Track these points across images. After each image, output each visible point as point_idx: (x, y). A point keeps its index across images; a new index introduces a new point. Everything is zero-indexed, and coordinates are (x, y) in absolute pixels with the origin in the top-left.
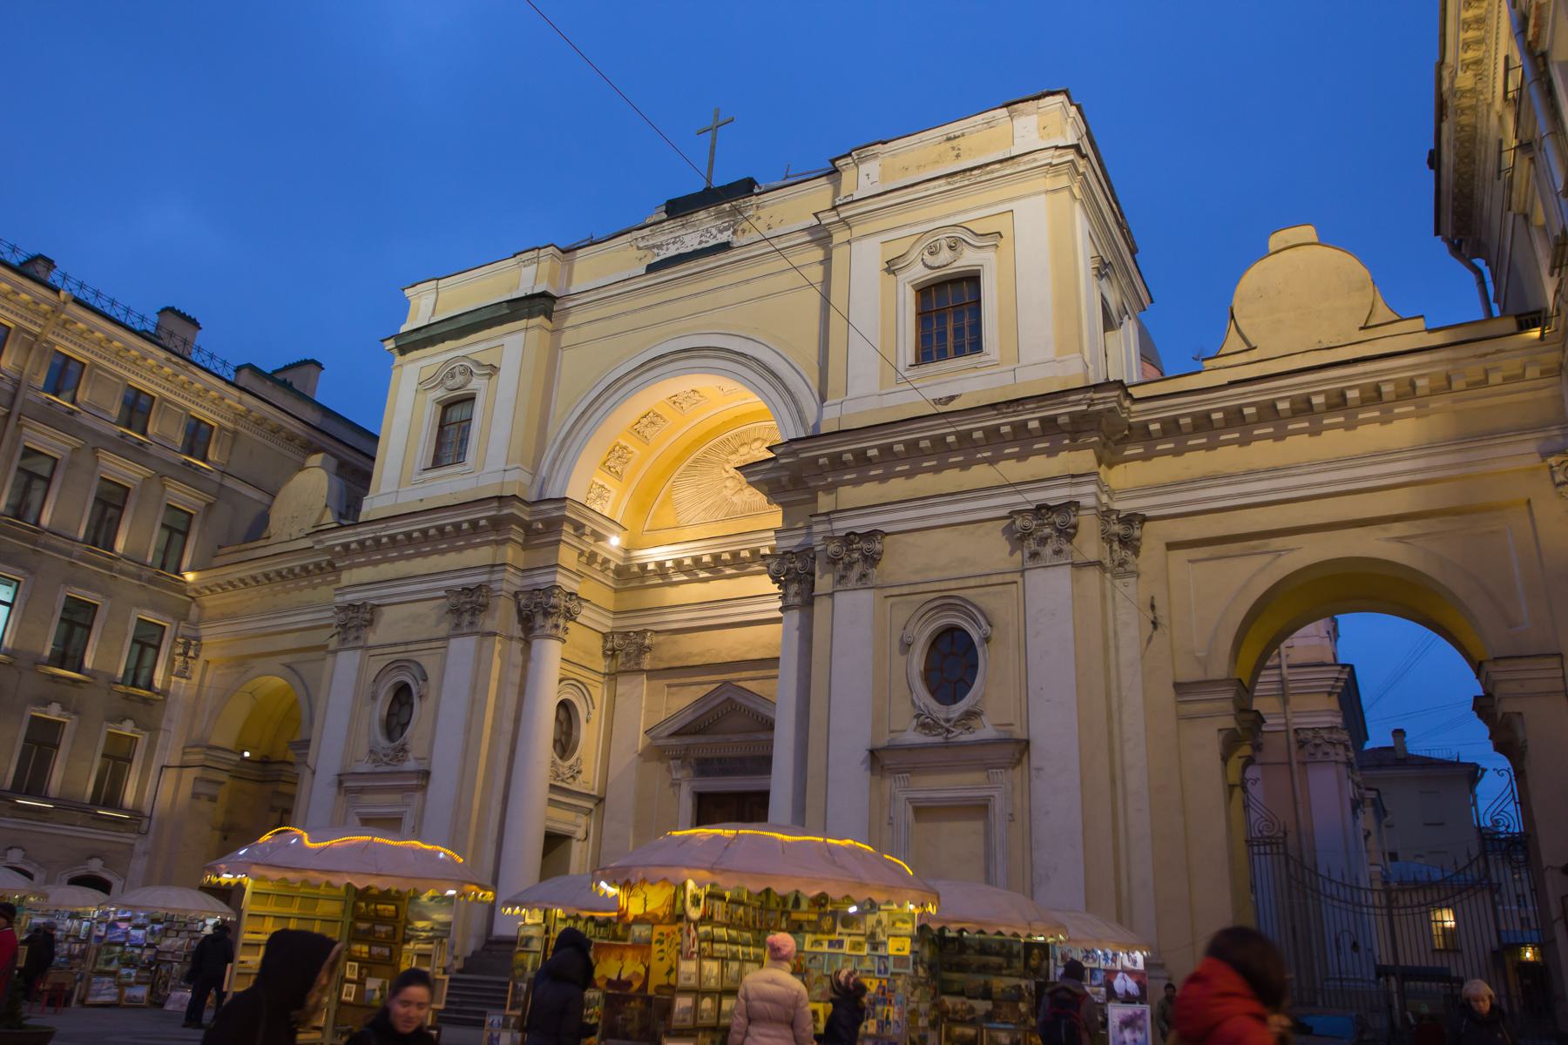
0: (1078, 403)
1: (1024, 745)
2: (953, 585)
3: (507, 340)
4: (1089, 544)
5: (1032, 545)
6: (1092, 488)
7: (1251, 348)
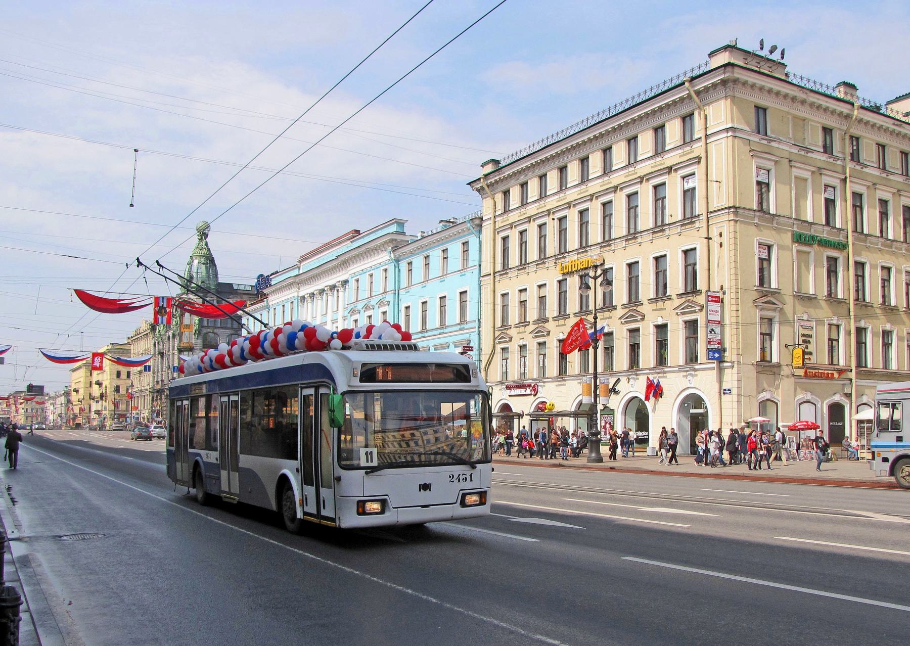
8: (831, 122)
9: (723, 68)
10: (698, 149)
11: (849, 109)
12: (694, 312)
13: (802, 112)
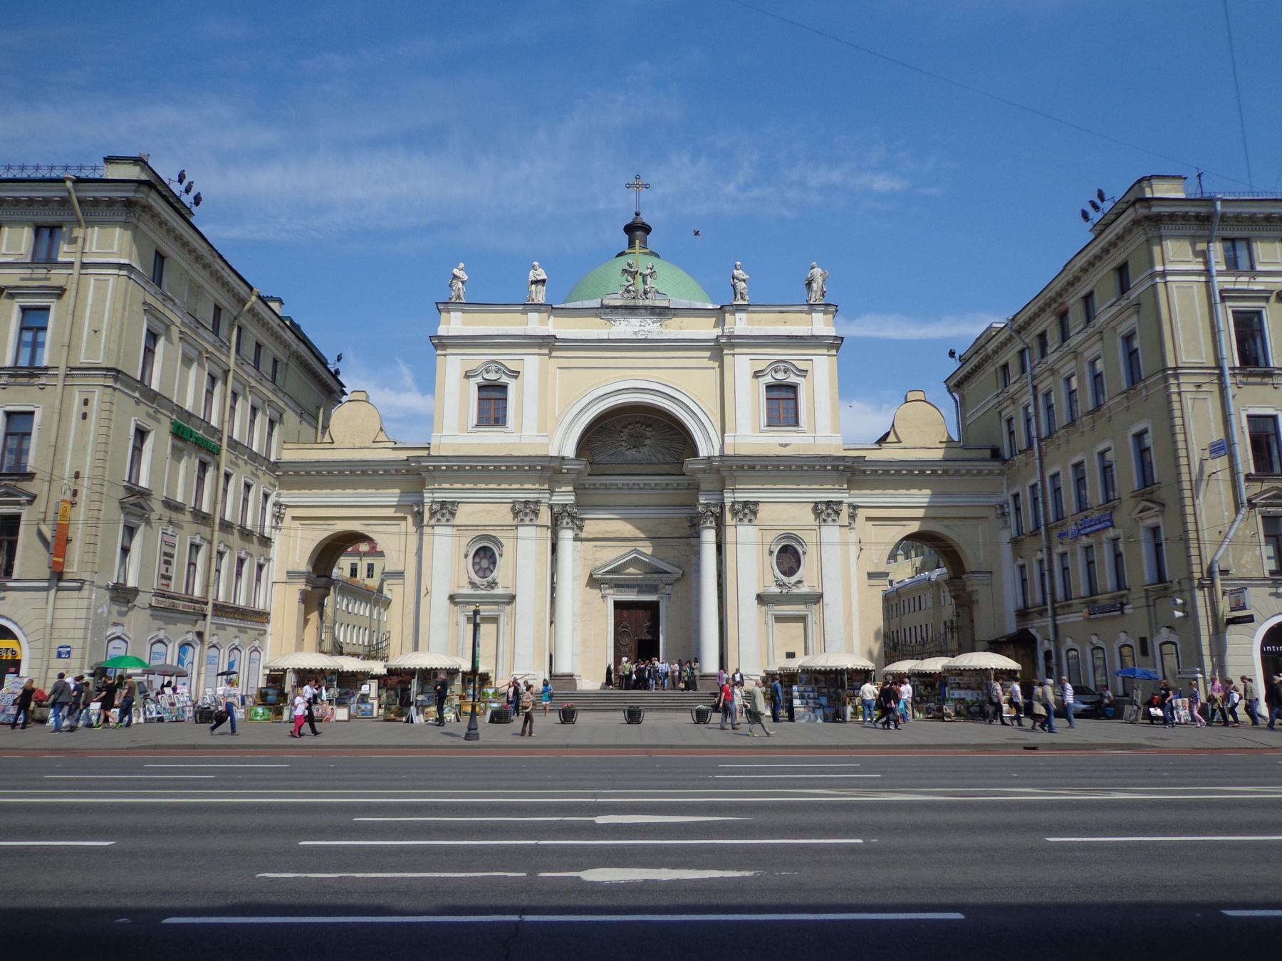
2: (789, 528)
4: (844, 518)
7: (899, 442)
8: (226, 302)
9: (136, 184)
10: (57, 277)
11: (245, 291)
12: (18, 503)
13: (201, 277)
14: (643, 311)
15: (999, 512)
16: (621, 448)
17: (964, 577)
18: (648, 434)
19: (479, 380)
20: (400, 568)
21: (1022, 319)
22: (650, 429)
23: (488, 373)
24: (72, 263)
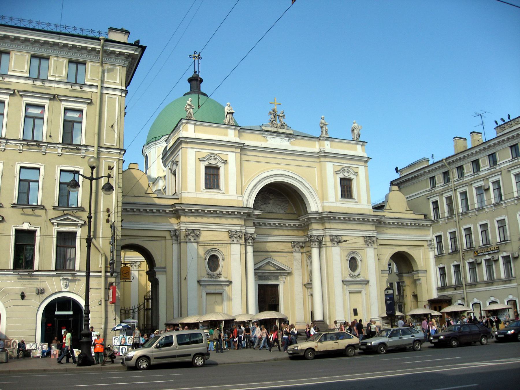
0: (378, 218)
1: (368, 281)
3: (229, 153)
5: (368, 243)
6: (376, 234)
12: (76, 225)
14: (282, 135)
15: (429, 243)
16: (259, 204)
17: (413, 273)
18: (271, 197)
19: (206, 163)
20: (163, 266)
21: (450, 160)
22: (272, 195)
23: (211, 160)
24: (97, 86)
